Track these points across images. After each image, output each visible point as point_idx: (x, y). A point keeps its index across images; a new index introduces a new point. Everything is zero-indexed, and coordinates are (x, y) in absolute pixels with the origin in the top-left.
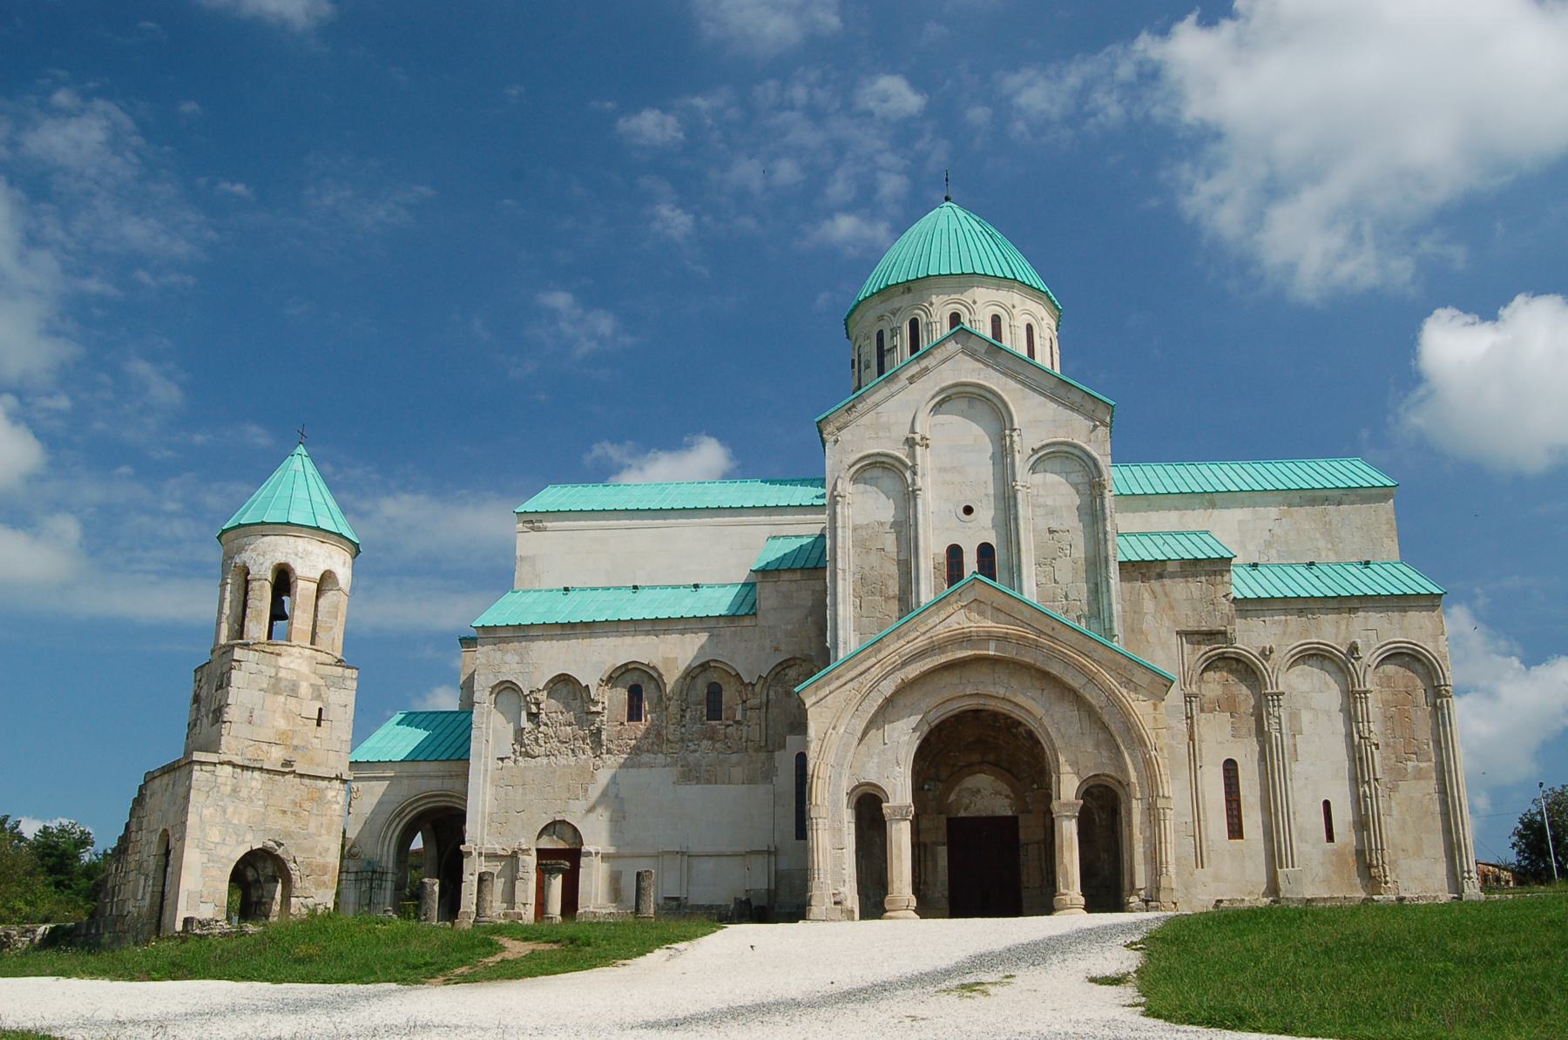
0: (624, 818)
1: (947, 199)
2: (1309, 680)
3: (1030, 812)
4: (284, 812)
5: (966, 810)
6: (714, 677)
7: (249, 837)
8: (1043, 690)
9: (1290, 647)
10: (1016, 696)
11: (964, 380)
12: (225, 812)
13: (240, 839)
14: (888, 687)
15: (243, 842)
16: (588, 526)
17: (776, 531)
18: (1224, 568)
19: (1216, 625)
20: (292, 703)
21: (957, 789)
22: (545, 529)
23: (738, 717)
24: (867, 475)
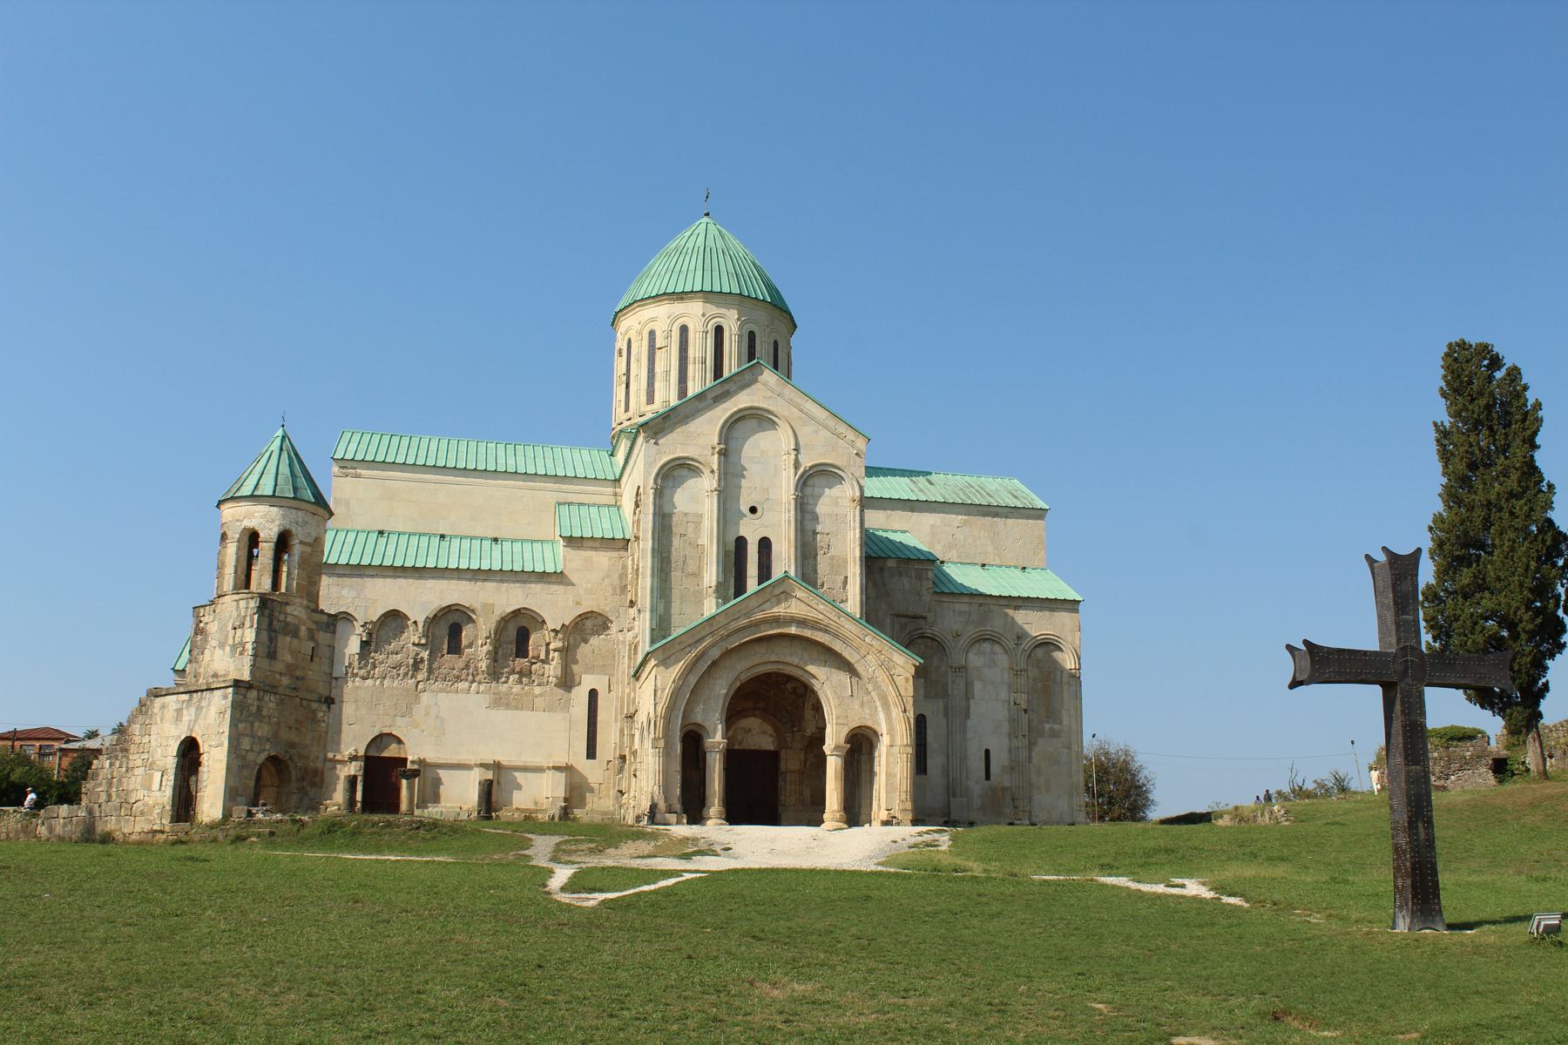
0: (444, 735)
1: (707, 214)
2: (982, 658)
3: (791, 748)
4: (290, 728)
5: (740, 743)
6: (524, 623)
7: (267, 747)
8: (826, 662)
9: (971, 633)
10: (806, 665)
11: (756, 404)
12: (252, 724)
13: (262, 748)
14: (715, 653)
15: (264, 750)
16: (388, 476)
17: (562, 497)
18: (929, 568)
19: (919, 612)
20: (296, 640)
21: (733, 728)
22: (358, 476)
23: (543, 657)
24: (676, 473)
